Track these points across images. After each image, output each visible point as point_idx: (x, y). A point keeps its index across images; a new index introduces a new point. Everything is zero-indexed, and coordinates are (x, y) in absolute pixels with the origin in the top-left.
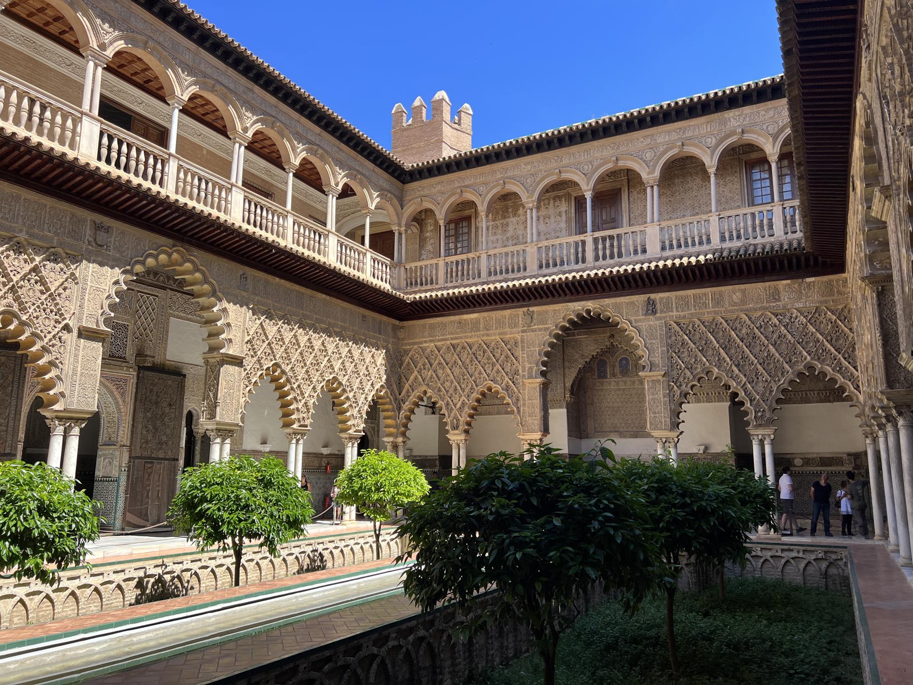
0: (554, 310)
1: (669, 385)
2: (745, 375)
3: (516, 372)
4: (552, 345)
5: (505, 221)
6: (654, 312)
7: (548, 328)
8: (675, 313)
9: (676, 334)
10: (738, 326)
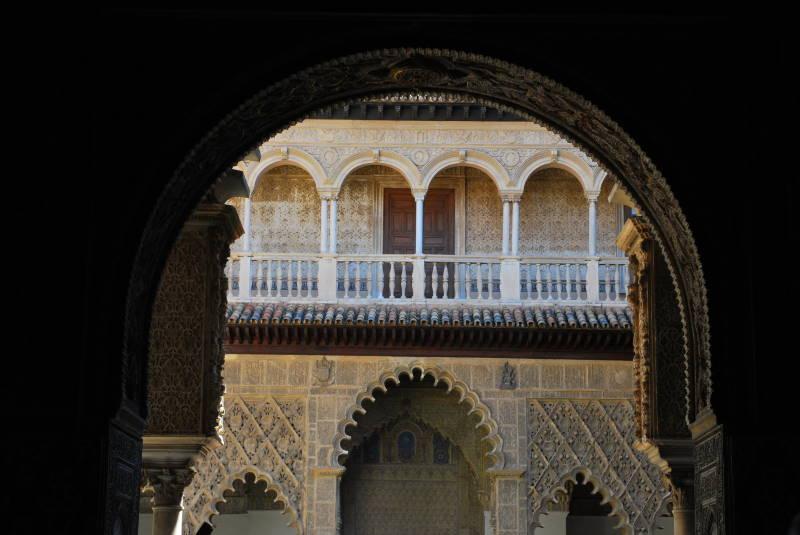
0: (366, 364)
1: (528, 489)
2: (625, 482)
3: (298, 455)
4: (357, 415)
5: (268, 204)
6: (513, 385)
7: (355, 391)
8: (540, 389)
9: (541, 419)
10: (620, 416)
